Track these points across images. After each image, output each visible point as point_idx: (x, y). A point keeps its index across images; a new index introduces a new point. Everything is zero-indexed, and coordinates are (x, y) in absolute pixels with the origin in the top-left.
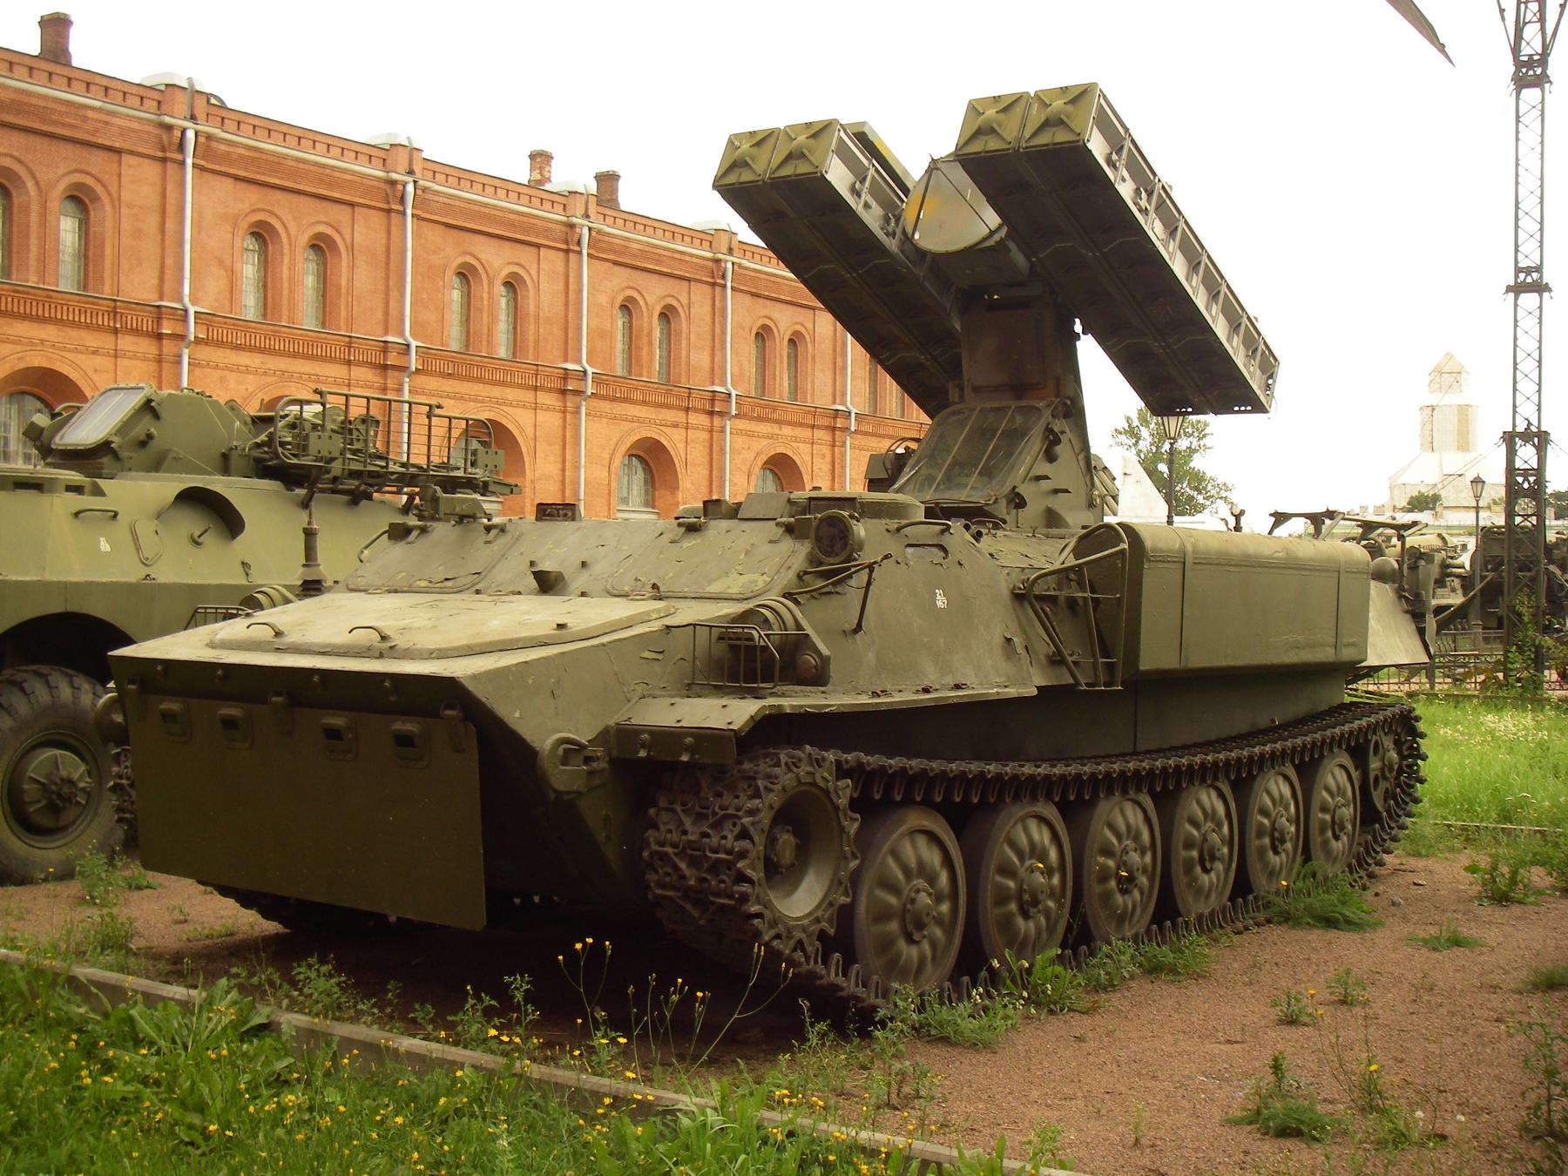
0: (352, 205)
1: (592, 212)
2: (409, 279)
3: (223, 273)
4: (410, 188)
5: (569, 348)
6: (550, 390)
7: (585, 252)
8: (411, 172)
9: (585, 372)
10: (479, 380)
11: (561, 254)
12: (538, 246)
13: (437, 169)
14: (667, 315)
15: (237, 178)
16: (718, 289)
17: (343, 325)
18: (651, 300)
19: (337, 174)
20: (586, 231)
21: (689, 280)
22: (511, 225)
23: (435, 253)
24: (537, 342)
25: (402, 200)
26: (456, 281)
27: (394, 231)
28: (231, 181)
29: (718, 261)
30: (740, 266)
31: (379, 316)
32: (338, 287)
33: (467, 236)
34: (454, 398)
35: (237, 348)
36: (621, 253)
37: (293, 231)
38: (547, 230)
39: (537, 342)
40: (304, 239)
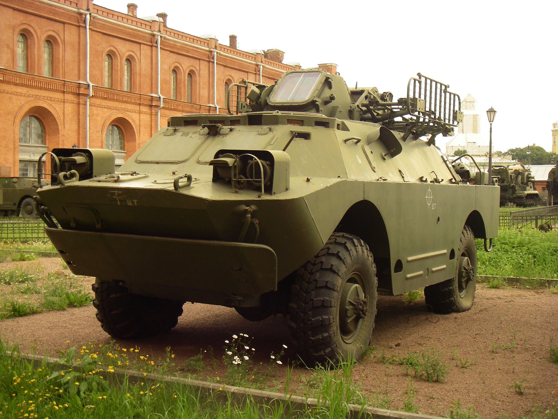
0: (64, 23)
1: (162, 30)
2: (88, 56)
3: (9, 51)
4: (88, 17)
5: (153, 87)
6: (146, 105)
7: (159, 47)
8: (88, 10)
9: (160, 98)
10: (117, 100)
11: (149, 47)
12: (140, 44)
13: (100, 9)
14: (191, 74)
15: (14, 9)
16: (211, 63)
17: (61, 76)
18: (185, 67)
19: (57, 9)
20: (159, 38)
21: (199, 59)
22: (129, 34)
23: (98, 45)
24: (140, 85)
25: (85, 22)
26: (106, 58)
27: (82, 36)
28: (12, 10)
29: (211, 52)
30: (220, 54)
31: (76, 72)
32: (59, 59)
33: (111, 38)
34: (107, 108)
35: (16, 84)
36: (173, 48)
37: (39, 34)
38: (144, 37)
39: (140, 85)
40: (44, 37)
